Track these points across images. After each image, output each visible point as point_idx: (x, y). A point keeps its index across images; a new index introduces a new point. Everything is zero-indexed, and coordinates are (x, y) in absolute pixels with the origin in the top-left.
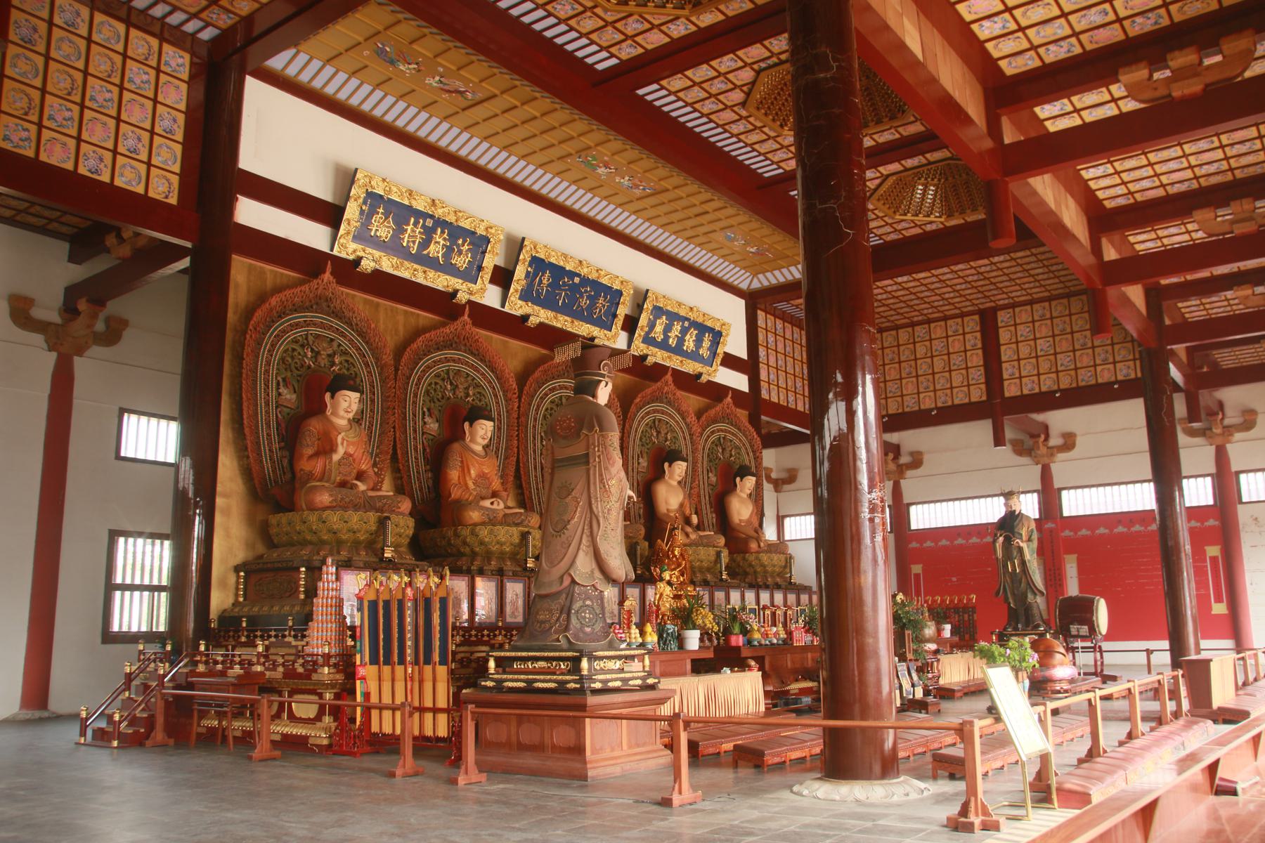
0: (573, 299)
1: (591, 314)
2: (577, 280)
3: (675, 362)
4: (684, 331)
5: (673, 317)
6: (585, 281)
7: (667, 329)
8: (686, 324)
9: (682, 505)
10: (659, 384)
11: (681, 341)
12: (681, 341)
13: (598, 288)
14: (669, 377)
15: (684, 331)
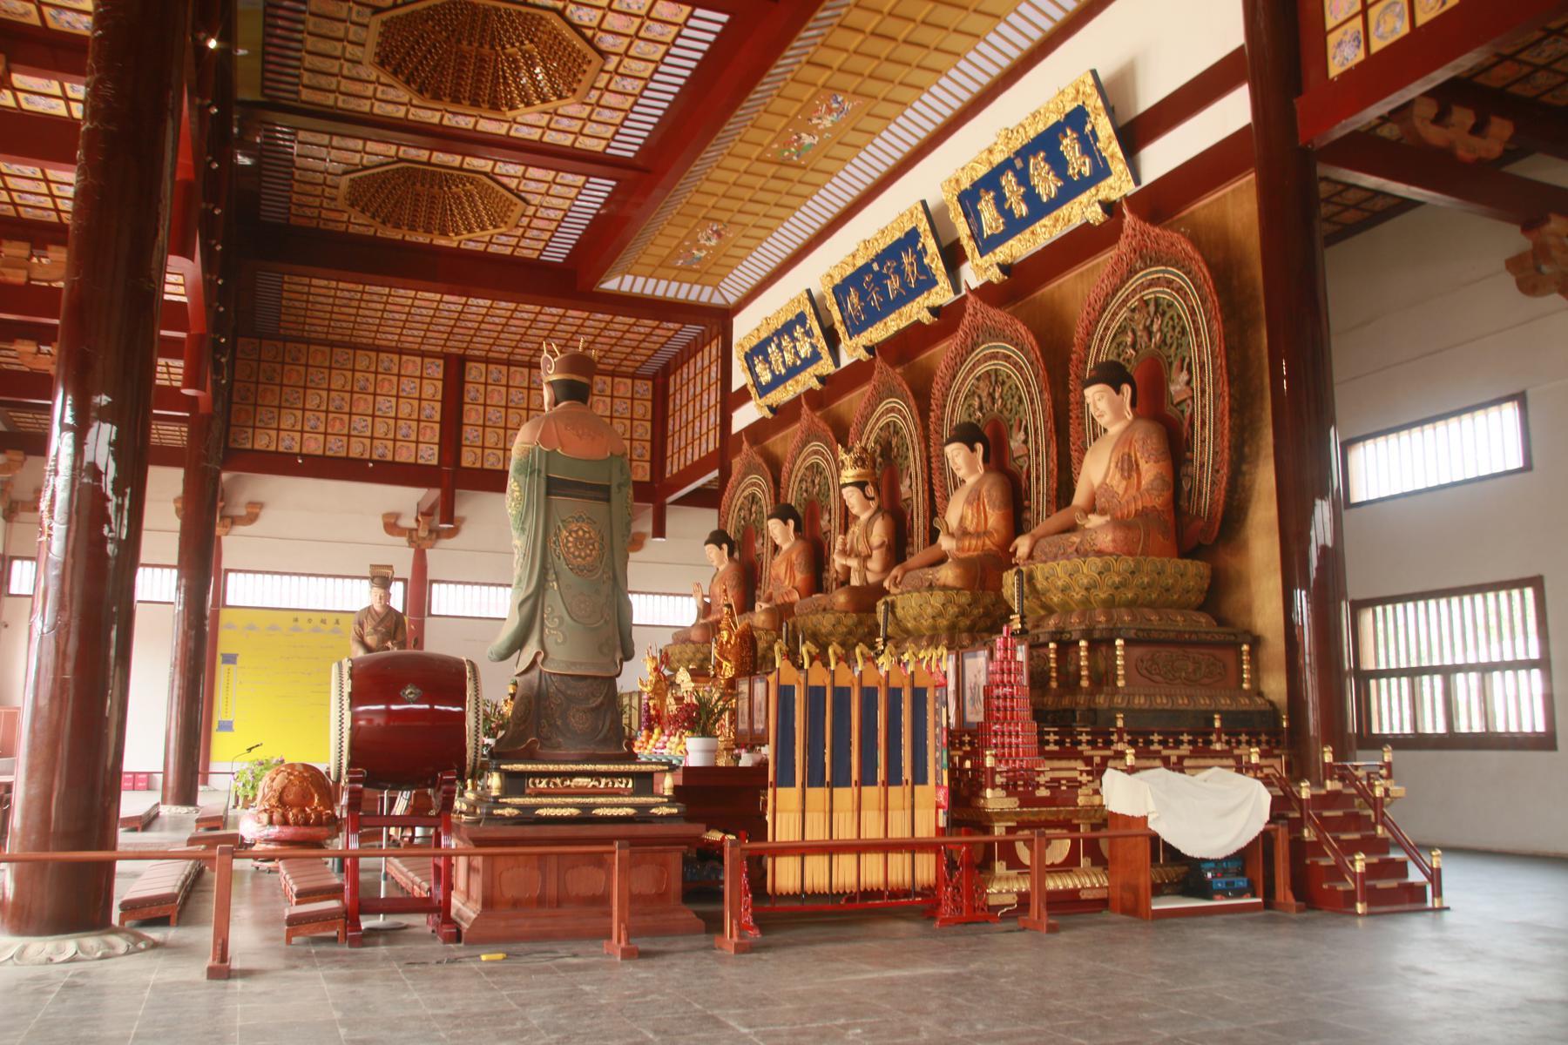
0: (884, 291)
1: (908, 290)
2: (875, 267)
3: (1045, 233)
4: (1023, 178)
5: (991, 181)
6: (881, 258)
7: (1000, 200)
8: (1019, 164)
9: (962, 519)
10: (967, 319)
11: (1031, 197)
12: (1031, 197)
13: (892, 253)
14: (971, 298)
15: (1023, 178)
